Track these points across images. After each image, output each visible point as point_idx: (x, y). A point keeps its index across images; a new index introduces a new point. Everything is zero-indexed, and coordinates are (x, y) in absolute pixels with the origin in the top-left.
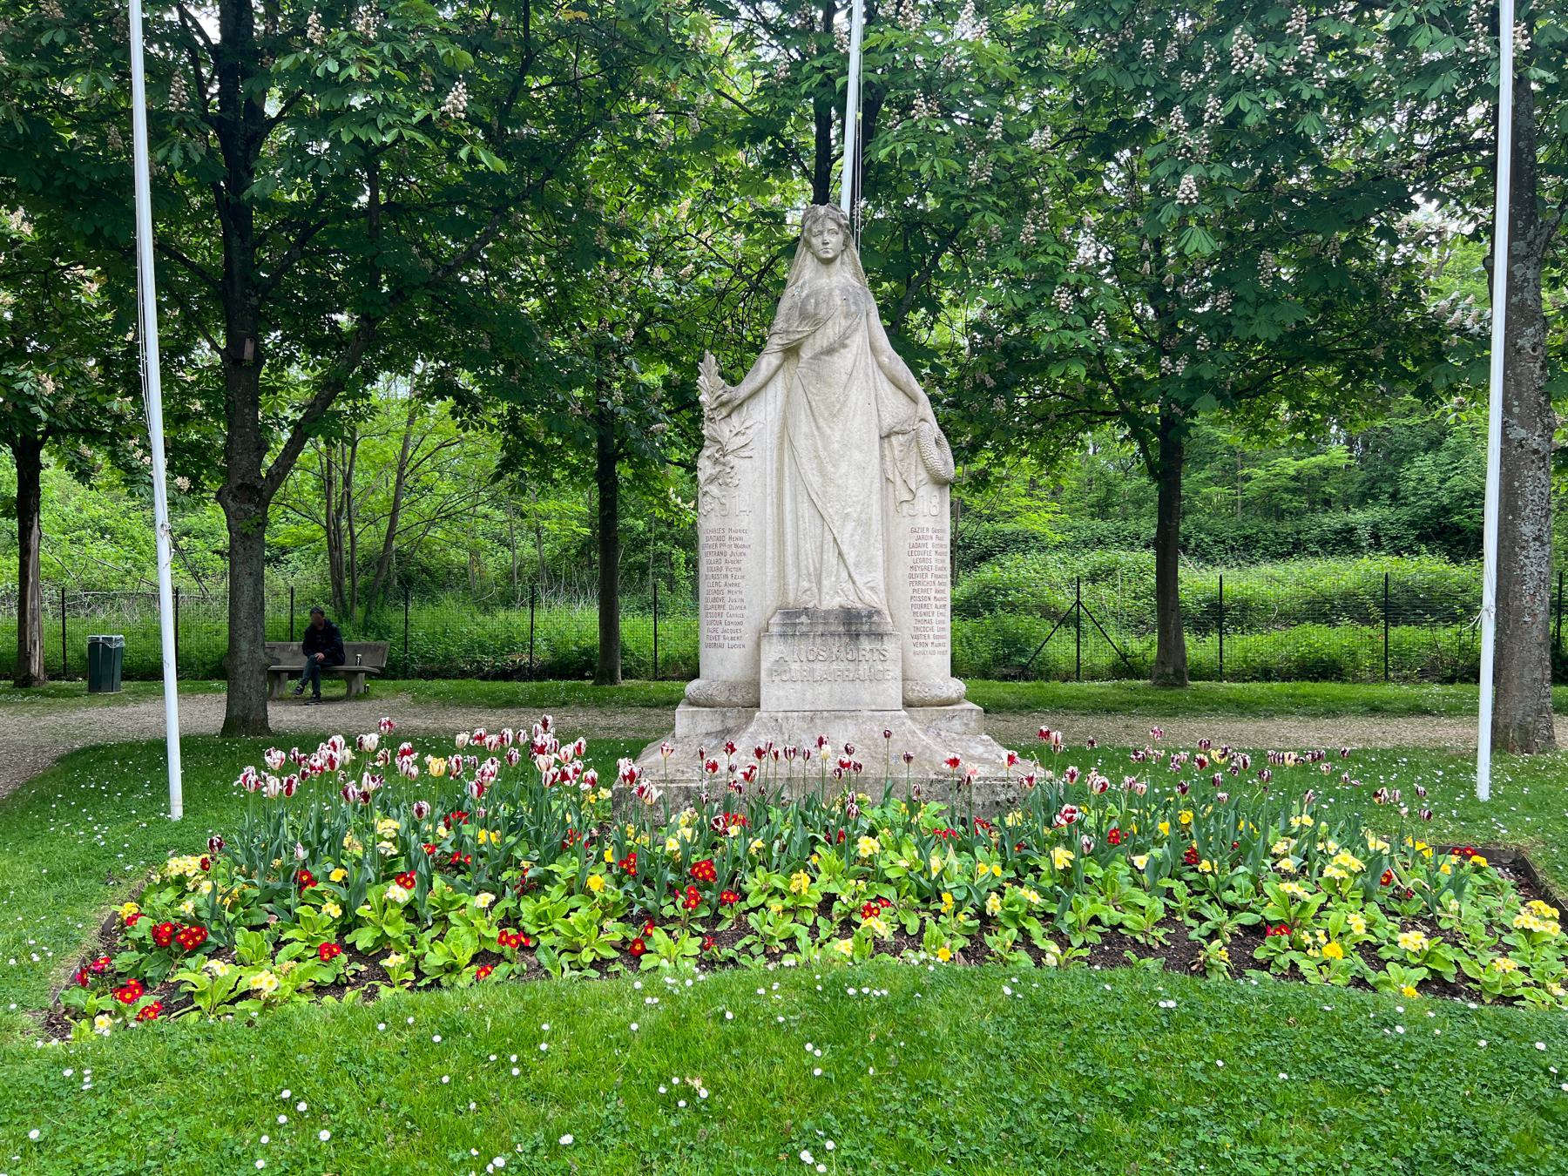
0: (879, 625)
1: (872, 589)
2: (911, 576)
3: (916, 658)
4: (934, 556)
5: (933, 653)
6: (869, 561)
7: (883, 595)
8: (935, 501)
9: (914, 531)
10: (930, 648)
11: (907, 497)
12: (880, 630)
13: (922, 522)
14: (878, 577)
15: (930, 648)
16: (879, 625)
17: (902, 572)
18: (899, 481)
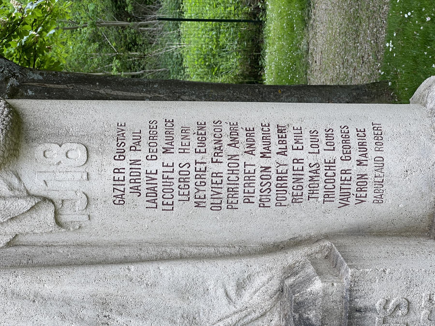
0: (326, 312)
1: (240, 287)
2: (216, 207)
3: (388, 198)
4: (175, 158)
5: (380, 163)
6: (183, 292)
7: (255, 264)
8: (55, 152)
9: (120, 200)
10: (369, 169)
11: (47, 214)
12: (339, 308)
13: (102, 185)
14: (216, 275)
15: (369, 169)
16: (326, 312)
17: (210, 226)
18: (14, 228)
